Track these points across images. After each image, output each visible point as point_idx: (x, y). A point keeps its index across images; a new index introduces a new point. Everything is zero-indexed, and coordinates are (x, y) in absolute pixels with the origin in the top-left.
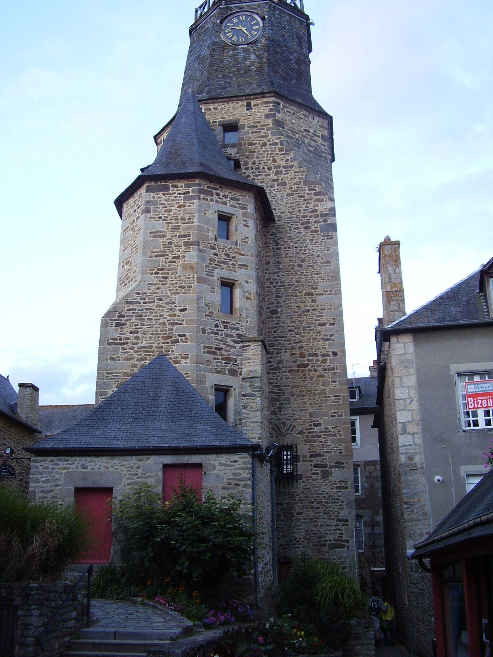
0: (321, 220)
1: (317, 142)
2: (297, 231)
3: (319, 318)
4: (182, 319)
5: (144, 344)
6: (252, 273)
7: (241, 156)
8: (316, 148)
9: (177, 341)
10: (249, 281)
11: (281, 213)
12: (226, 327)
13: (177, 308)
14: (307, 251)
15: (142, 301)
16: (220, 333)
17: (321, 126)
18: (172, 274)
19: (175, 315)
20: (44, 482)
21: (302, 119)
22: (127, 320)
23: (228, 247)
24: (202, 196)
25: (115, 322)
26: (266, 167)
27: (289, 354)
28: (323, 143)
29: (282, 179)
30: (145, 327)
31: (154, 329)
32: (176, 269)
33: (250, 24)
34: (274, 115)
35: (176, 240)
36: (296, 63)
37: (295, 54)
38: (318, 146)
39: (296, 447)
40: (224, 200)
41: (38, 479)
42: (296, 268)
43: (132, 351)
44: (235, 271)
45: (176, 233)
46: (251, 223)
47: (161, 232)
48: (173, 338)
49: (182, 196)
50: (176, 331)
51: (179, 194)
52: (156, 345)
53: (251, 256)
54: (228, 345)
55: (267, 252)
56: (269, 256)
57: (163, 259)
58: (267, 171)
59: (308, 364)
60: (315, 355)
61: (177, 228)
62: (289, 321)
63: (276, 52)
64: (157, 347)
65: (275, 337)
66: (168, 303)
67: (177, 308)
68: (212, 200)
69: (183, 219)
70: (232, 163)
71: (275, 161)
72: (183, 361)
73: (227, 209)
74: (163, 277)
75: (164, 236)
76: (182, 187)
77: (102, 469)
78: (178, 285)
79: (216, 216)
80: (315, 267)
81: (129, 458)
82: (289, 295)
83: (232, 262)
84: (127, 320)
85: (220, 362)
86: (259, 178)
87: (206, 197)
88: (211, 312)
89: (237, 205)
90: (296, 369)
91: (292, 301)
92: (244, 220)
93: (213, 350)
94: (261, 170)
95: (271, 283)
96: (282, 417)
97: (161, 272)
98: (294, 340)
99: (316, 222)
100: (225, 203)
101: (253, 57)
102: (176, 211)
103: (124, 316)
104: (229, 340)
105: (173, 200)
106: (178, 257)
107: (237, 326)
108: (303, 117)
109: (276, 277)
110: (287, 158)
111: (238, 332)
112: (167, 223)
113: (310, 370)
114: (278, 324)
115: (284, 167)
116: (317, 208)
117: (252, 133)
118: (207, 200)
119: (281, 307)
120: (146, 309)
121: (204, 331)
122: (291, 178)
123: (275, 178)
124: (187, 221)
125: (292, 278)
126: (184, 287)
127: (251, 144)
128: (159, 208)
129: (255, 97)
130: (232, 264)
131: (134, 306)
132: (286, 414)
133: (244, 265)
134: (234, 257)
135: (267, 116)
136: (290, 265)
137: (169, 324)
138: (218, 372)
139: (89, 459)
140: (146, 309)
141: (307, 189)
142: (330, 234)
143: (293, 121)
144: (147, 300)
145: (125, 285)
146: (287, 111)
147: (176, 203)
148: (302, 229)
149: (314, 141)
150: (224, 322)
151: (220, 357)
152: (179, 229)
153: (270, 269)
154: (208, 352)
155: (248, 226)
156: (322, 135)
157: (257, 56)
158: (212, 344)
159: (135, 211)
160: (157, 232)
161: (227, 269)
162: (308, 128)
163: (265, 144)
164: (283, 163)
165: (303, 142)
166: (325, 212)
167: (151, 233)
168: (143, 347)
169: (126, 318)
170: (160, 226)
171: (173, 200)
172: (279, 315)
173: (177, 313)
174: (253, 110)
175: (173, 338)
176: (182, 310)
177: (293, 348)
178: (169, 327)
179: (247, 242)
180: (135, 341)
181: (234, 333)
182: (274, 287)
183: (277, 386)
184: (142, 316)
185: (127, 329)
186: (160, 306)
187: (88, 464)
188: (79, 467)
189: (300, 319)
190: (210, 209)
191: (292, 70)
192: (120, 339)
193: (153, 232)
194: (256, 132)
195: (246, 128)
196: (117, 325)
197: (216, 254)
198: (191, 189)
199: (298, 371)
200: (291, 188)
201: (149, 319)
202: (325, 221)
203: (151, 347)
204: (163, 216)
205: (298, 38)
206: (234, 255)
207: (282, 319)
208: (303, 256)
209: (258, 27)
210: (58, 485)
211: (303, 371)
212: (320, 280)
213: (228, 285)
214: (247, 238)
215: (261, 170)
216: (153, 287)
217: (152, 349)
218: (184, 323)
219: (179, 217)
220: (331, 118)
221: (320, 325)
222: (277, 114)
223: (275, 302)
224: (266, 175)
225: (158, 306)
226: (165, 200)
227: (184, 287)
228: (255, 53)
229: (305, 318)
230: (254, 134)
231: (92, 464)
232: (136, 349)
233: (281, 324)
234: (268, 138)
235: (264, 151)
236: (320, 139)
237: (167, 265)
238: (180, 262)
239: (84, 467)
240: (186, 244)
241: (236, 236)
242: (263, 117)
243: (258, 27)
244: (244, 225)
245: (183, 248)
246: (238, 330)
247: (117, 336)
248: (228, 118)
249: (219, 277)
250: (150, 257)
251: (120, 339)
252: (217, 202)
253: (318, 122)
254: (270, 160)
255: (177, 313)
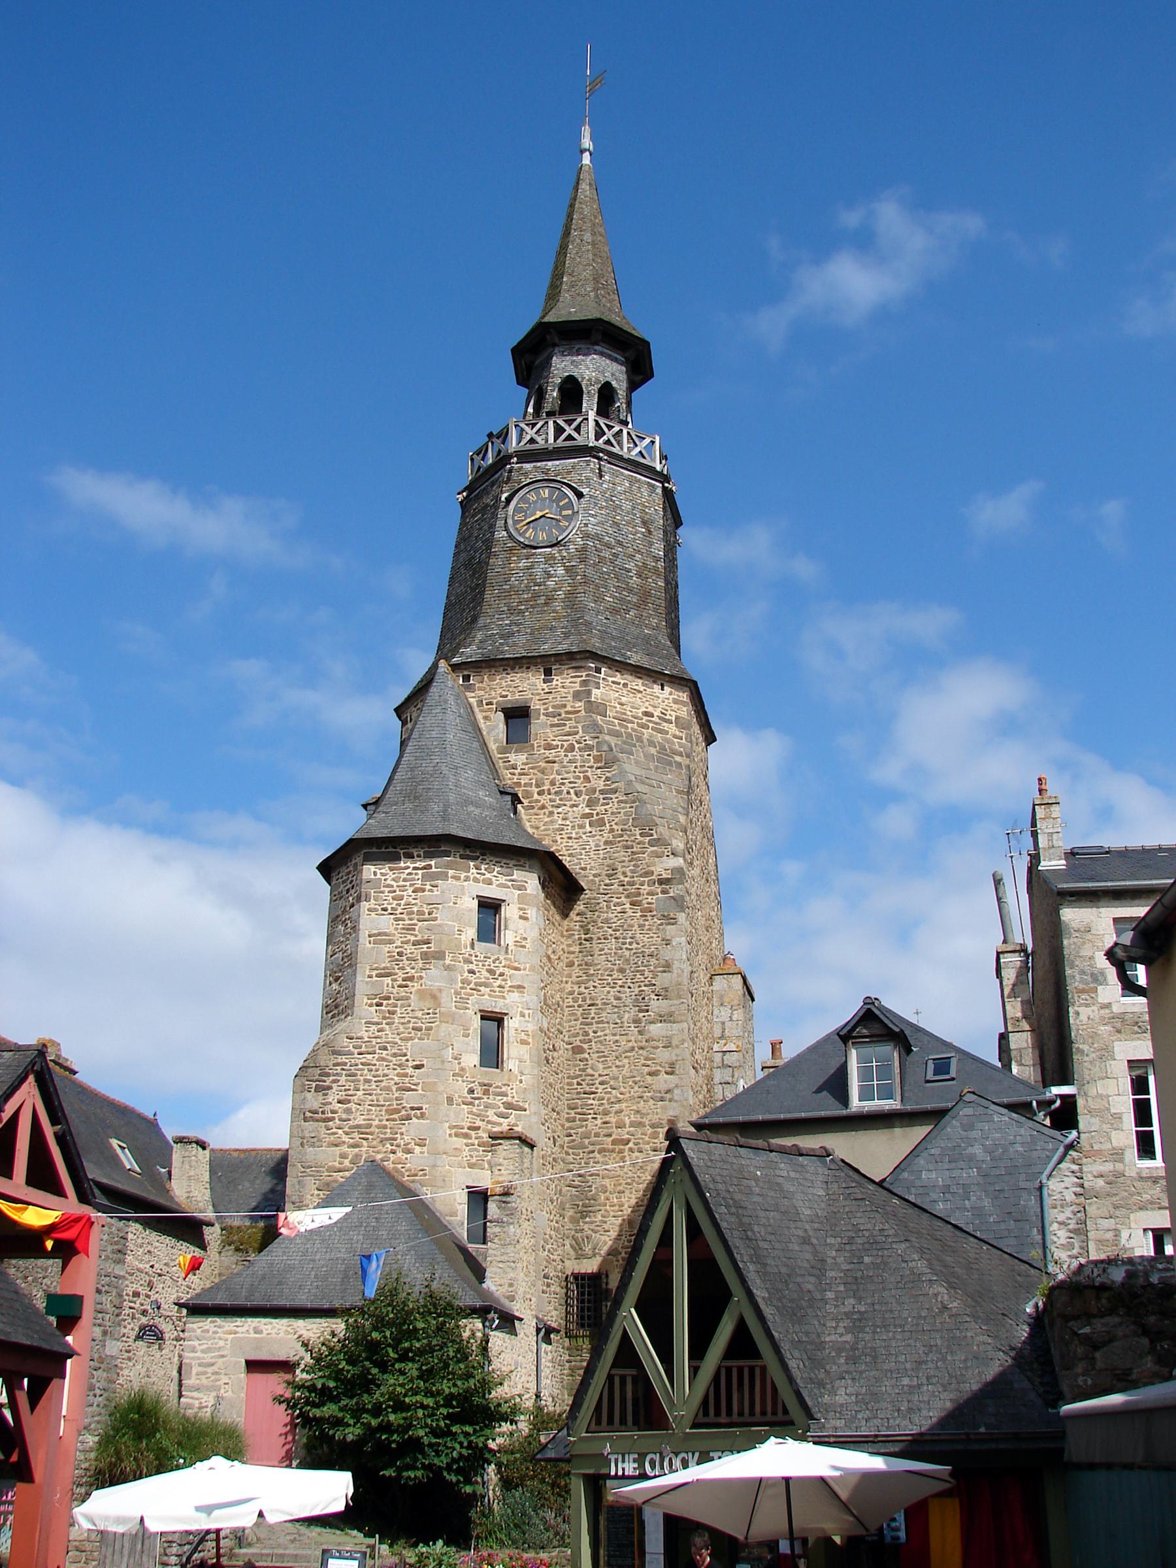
0: (659, 890)
1: (667, 733)
2: (619, 909)
3: (649, 1063)
4: (415, 1080)
5: (360, 1121)
6: (532, 998)
7: (532, 768)
8: (663, 748)
9: (409, 1118)
10: (527, 1012)
11: (595, 876)
12: (486, 1092)
13: (410, 1064)
14: (634, 946)
15: (356, 1051)
16: (477, 1102)
17: (676, 701)
18: (403, 1006)
19: (406, 1075)
20: (203, 1351)
21: (640, 692)
22: (334, 1081)
23: (493, 958)
24: (451, 872)
25: (314, 1084)
26: (572, 791)
27: (599, 1122)
28: (677, 733)
29: (598, 814)
30: (360, 1093)
31: (374, 1097)
32: (408, 998)
33: (558, 505)
34: (589, 693)
35: (409, 949)
36: (639, 576)
37: (638, 556)
38: (668, 741)
39: (607, 1276)
40: (488, 875)
41: (194, 1347)
42: (616, 975)
43: (340, 1131)
44: (504, 997)
45: (409, 937)
46: (532, 913)
47: (385, 934)
48: (403, 1112)
49: (420, 872)
50: (409, 1099)
51: (415, 868)
52: (377, 1122)
53: (532, 969)
54: (489, 1122)
55: (569, 945)
56: (573, 953)
57: (388, 980)
58: (574, 797)
59: (629, 1141)
60: (640, 1124)
61: (410, 929)
62: (601, 1066)
63: (602, 560)
64: (378, 1127)
65: (579, 1093)
66: (395, 1055)
67: (410, 1064)
68: (467, 879)
69: (421, 913)
70: (509, 798)
71: (587, 779)
72: (418, 1149)
73: (492, 892)
74: (389, 1012)
75: (391, 942)
76: (419, 856)
77: (282, 1334)
78: (411, 1025)
79: (475, 904)
80: (646, 973)
81: (318, 1320)
82: (602, 1022)
83: (498, 982)
84: (334, 1081)
85: (476, 1150)
86: (560, 810)
87: (457, 873)
88: (462, 1069)
89: (510, 884)
90: (611, 1147)
91: (607, 1032)
92: (521, 909)
93: (466, 1130)
94: (564, 795)
95: (575, 1000)
96: (586, 1227)
97: (385, 1002)
98: (609, 1099)
99: (651, 893)
100: (489, 882)
101: (561, 571)
102: (410, 899)
103: (328, 1075)
104: (490, 1112)
105: (405, 880)
106: (411, 979)
107: (504, 1089)
108: (642, 689)
109: (582, 989)
110: (608, 775)
111: (505, 1099)
112: (396, 920)
113: (631, 1150)
114: (584, 1070)
115: (602, 792)
116: (652, 868)
117: (552, 726)
118: (457, 878)
119: (590, 1041)
120: (362, 1064)
121: (450, 1100)
122: (612, 813)
123: (587, 811)
124: (427, 916)
125: (609, 992)
126: (420, 1029)
127: (549, 747)
128: (382, 892)
129: (558, 658)
130: (500, 986)
131: (343, 1059)
132: (592, 1223)
133: (519, 987)
134: (502, 974)
135: (577, 696)
136: (606, 970)
137: (398, 1089)
138: (471, 1166)
139: (263, 1320)
140: (362, 1064)
141: (638, 832)
142: (672, 916)
143: (624, 699)
144: (363, 1049)
145: (333, 1017)
146: (613, 682)
147: (411, 885)
148: (628, 906)
149: (661, 731)
150: (482, 1085)
151: (476, 1142)
152: (414, 930)
153: (574, 975)
154: (456, 1135)
155: (526, 919)
156: (677, 718)
157: (567, 569)
158: (463, 1120)
159: (348, 891)
160: (379, 934)
161: (490, 995)
162: (650, 709)
163: (571, 748)
164: (601, 784)
165: (640, 739)
166: (665, 876)
167: (370, 936)
168: (358, 1126)
169: (331, 1078)
170: (386, 923)
171: (405, 880)
172: (586, 1056)
173: (410, 1071)
174: (555, 682)
175: (403, 1112)
176: (417, 1067)
177: (606, 1113)
178: (397, 1095)
179: (524, 947)
180: (344, 1116)
181: (499, 1101)
182: (579, 1006)
183: (580, 1175)
184: (355, 1075)
185: (333, 1097)
186: (383, 1059)
187: (263, 1327)
188: (251, 1331)
189: (618, 1063)
190: (463, 894)
191: (630, 591)
192: (323, 1113)
193: (374, 935)
194: (558, 725)
195: (542, 717)
196: (318, 1089)
197: (472, 972)
198: (433, 863)
199: (613, 1151)
200: (612, 830)
201: (367, 1081)
202: (663, 892)
203: (370, 1126)
204: (389, 907)
205: (645, 523)
206: (501, 970)
207: (590, 1062)
208: (627, 953)
209: (570, 512)
210: (223, 1356)
211: (621, 1151)
212: (653, 996)
213: (495, 1019)
214: (525, 939)
215: (564, 795)
216: (374, 1027)
217: (372, 1129)
218: (419, 1087)
219: (415, 909)
220: (695, 683)
221: (650, 1074)
222: (595, 691)
223: (581, 1032)
224: (573, 806)
225: (379, 1059)
226: (393, 880)
227: (420, 1029)
228: (564, 565)
229: (626, 1061)
230: (555, 729)
231: (269, 1327)
232: (346, 1129)
233: (589, 1071)
234: (577, 737)
235: (570, 762)
236: (673, 726)
237: (395, 991)
238: (415, 986)
239: (257, 1331)
240: (425, 956)
241: (508, 937)
242: (570, 698)
243: (570, 512)
244: (521, 917)
245: (420, 964)
246: (506, 1095)
247: (316, 1105)
248: (514, 698)
249: (477, 1007)
250: (370, 977)
251: (323, 1113)
252: (476, 880)
253: (671, 694)
254: (579, 778)
255: (410, 1071)
